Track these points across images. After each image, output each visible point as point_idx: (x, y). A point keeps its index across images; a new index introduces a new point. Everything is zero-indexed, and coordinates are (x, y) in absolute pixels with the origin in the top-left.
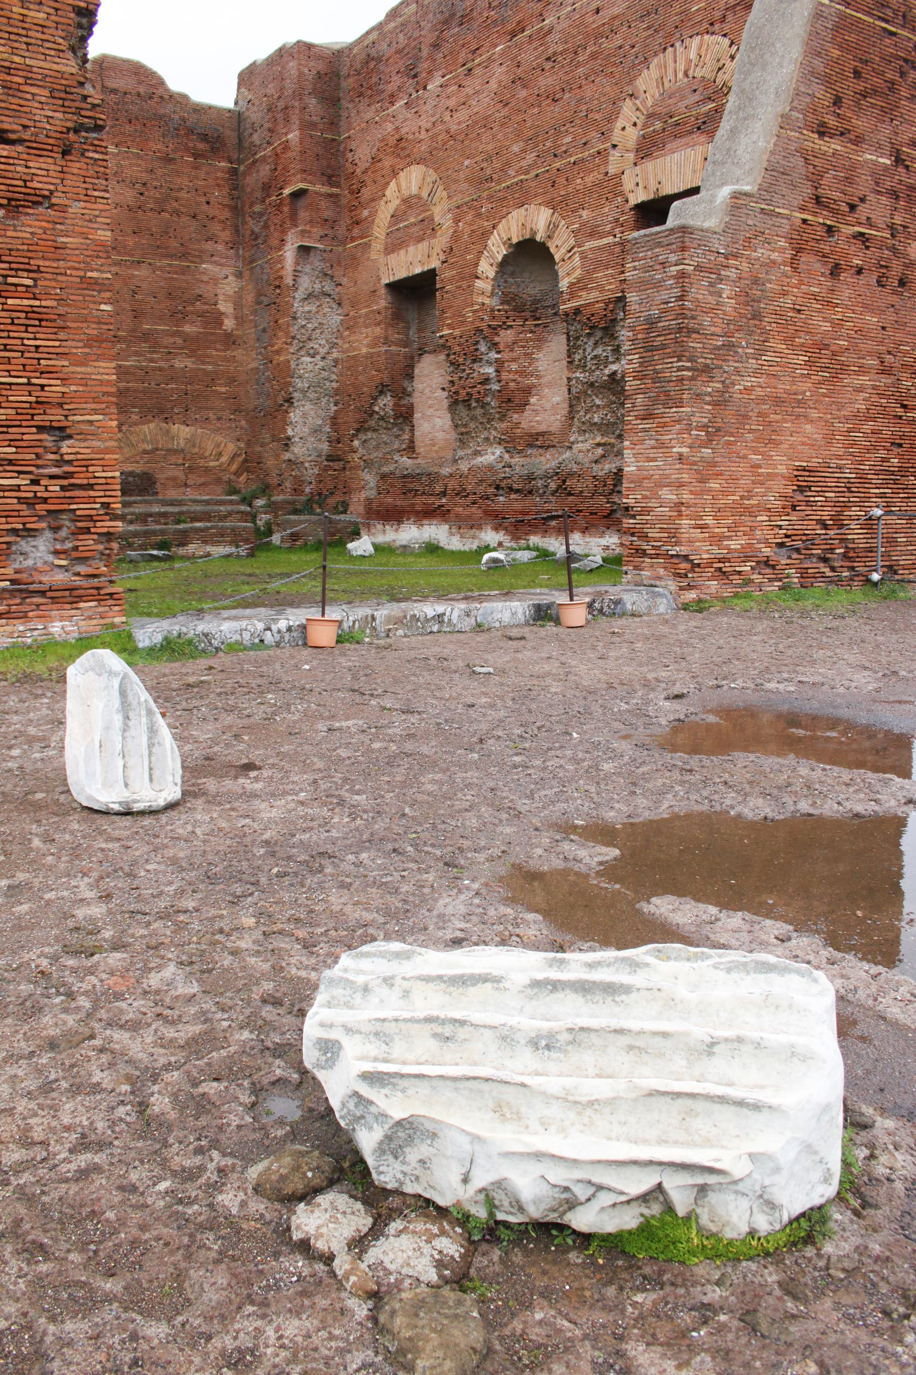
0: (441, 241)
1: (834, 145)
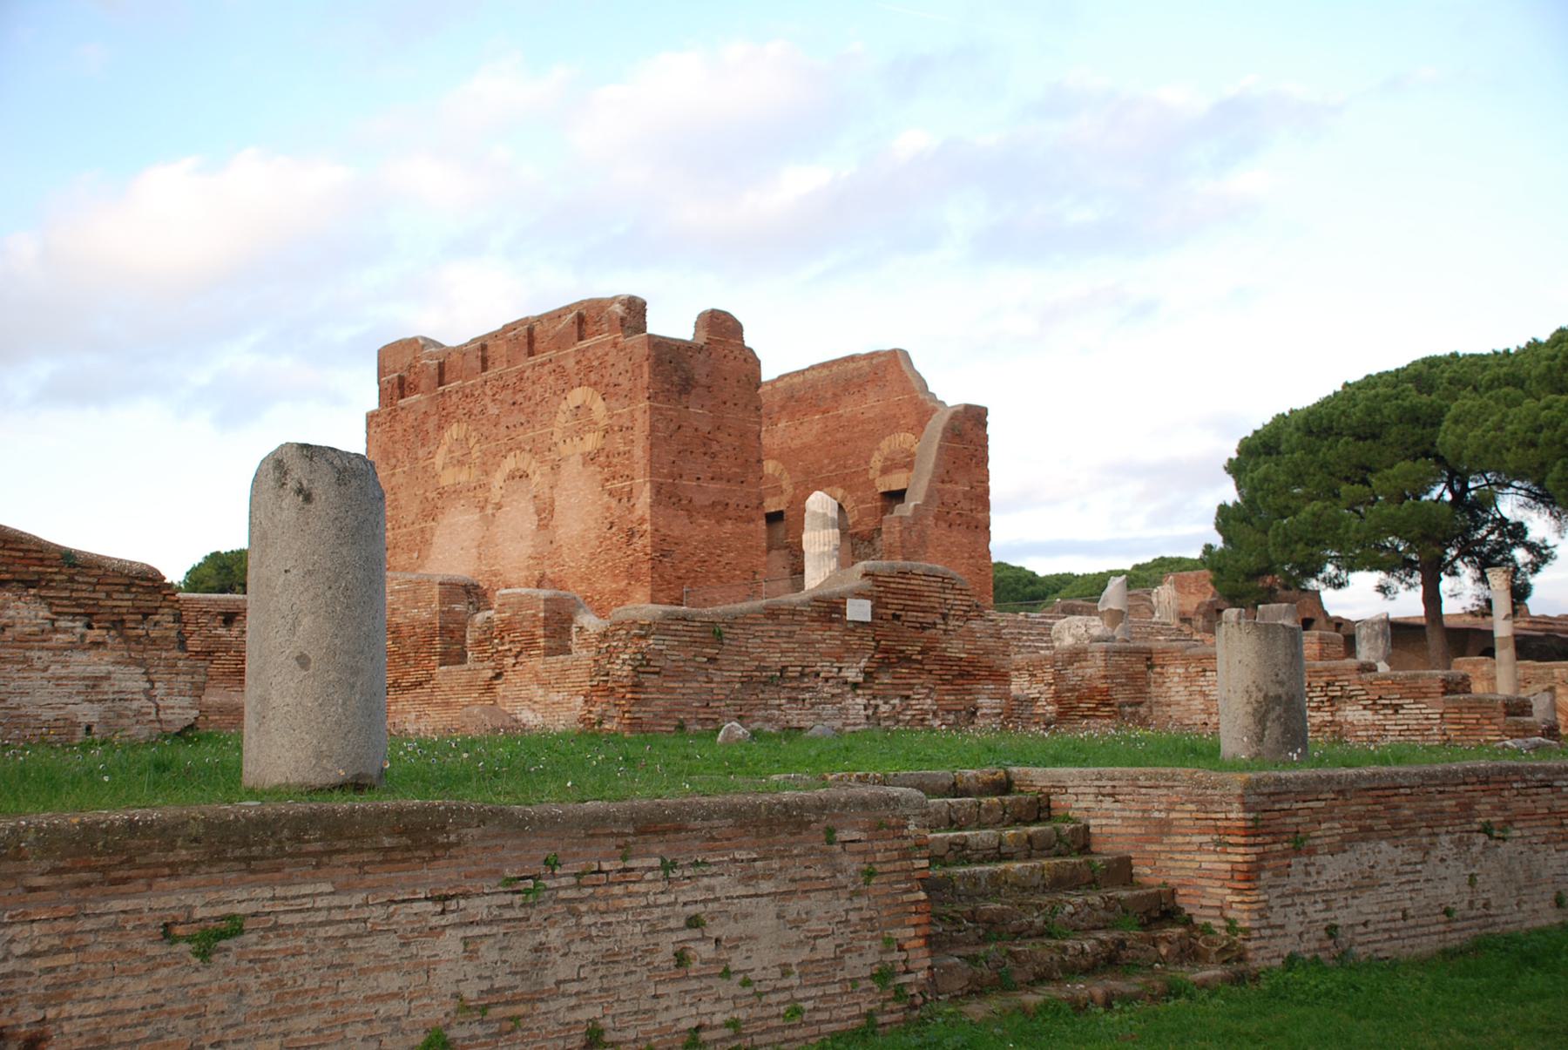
0: (785, 498)
1: (948, 486)
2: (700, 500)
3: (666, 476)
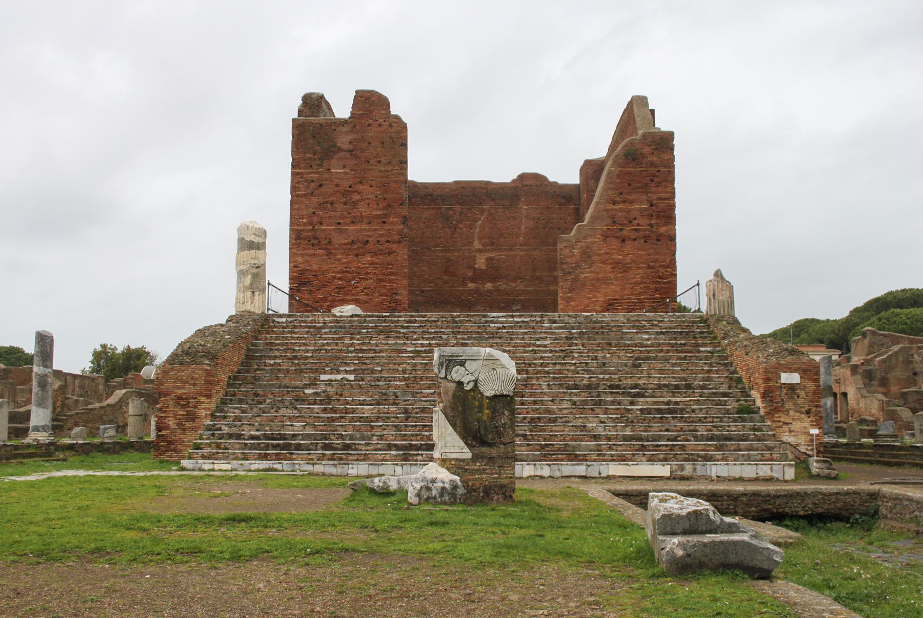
1: (620, 206)
2: (338, 240)
3: (305, 224)
